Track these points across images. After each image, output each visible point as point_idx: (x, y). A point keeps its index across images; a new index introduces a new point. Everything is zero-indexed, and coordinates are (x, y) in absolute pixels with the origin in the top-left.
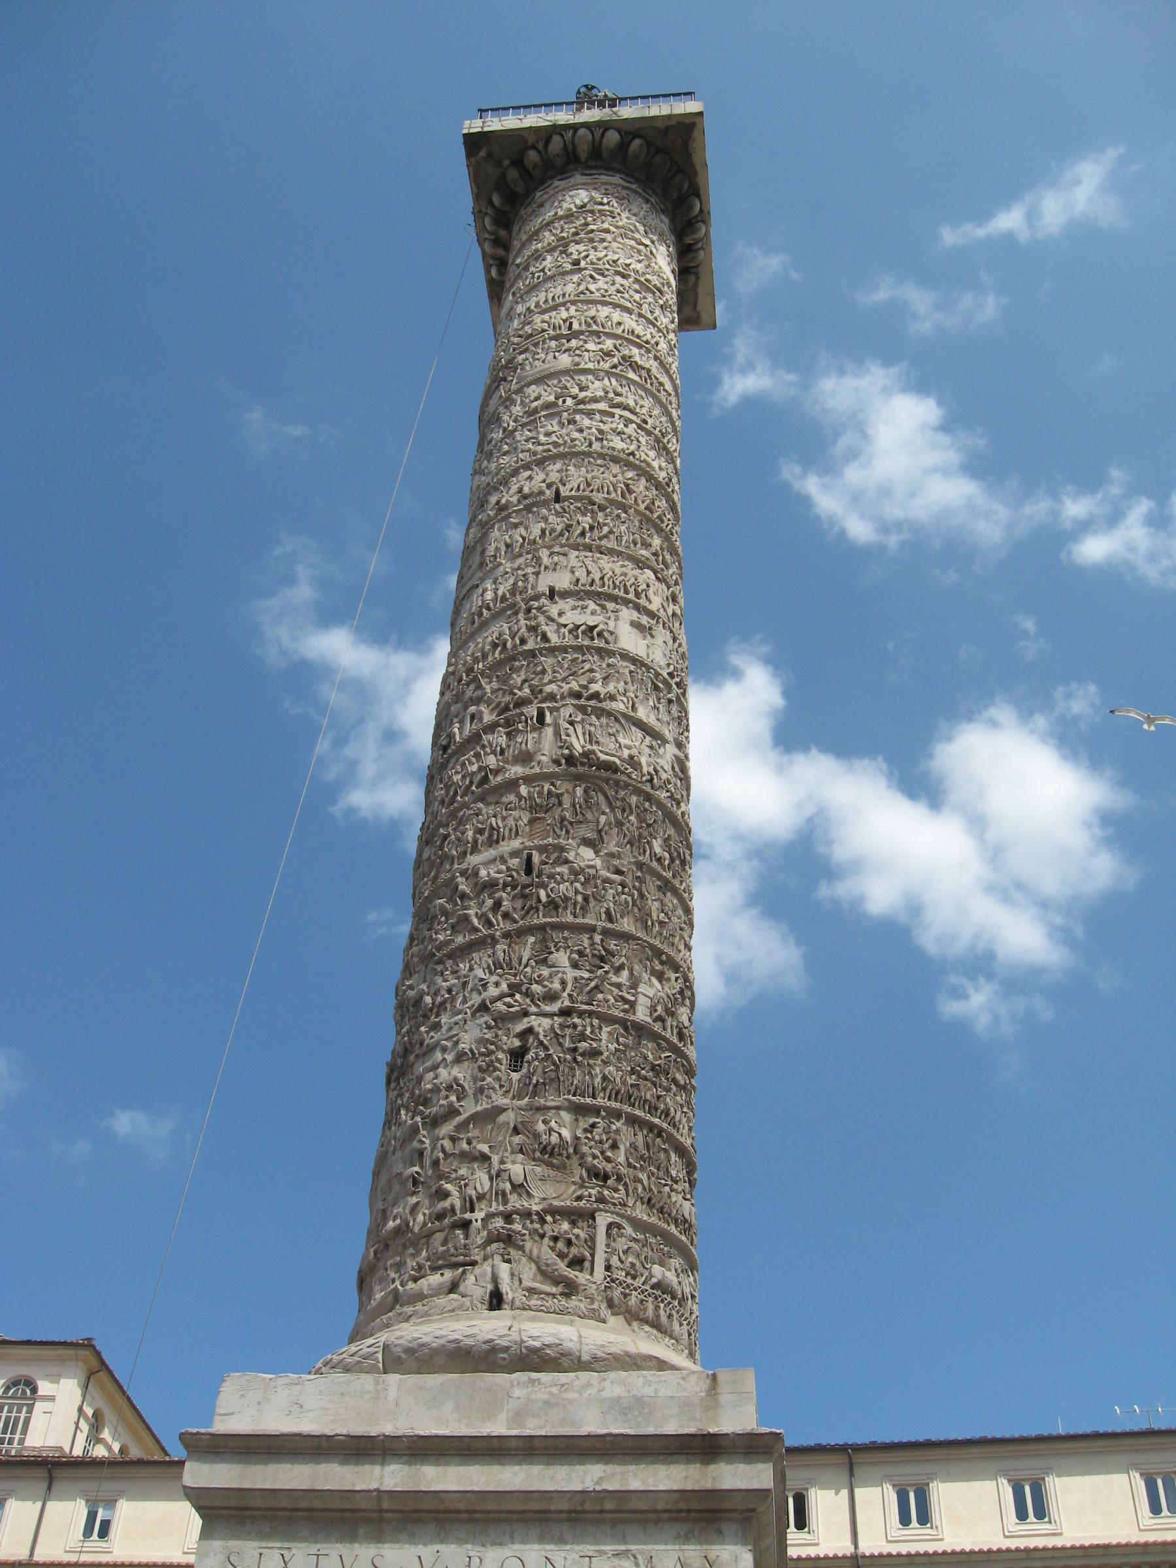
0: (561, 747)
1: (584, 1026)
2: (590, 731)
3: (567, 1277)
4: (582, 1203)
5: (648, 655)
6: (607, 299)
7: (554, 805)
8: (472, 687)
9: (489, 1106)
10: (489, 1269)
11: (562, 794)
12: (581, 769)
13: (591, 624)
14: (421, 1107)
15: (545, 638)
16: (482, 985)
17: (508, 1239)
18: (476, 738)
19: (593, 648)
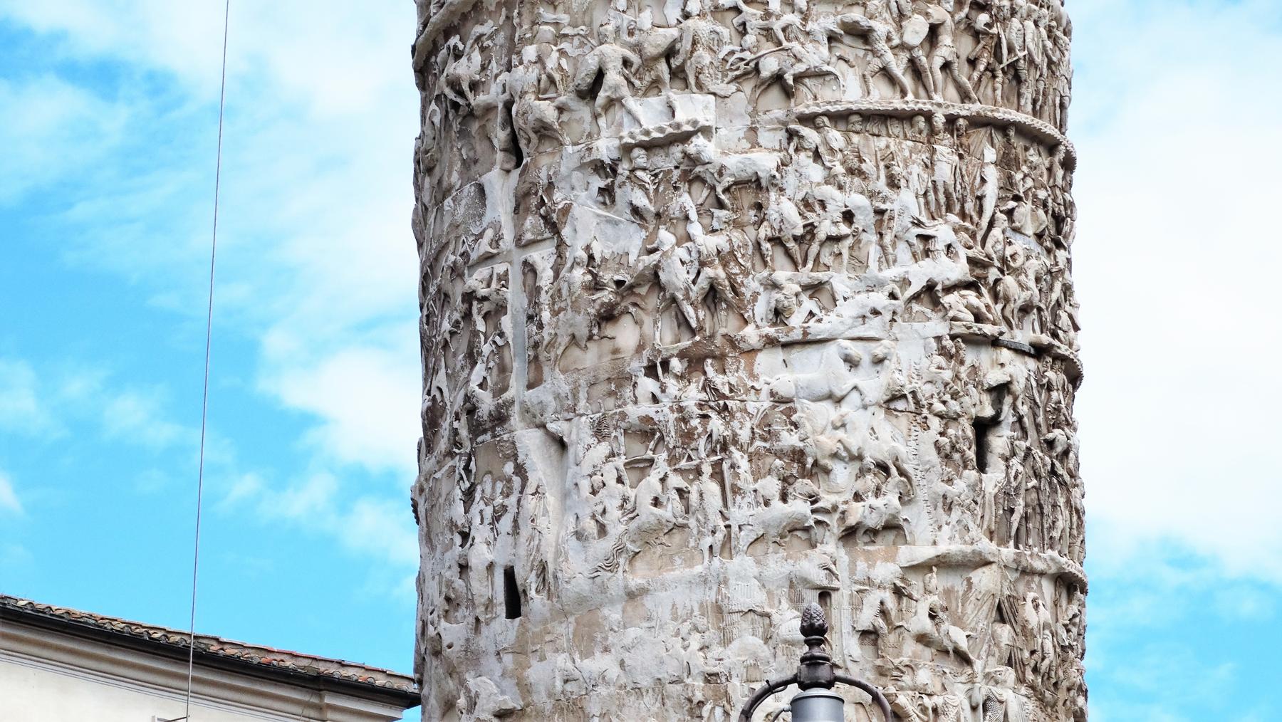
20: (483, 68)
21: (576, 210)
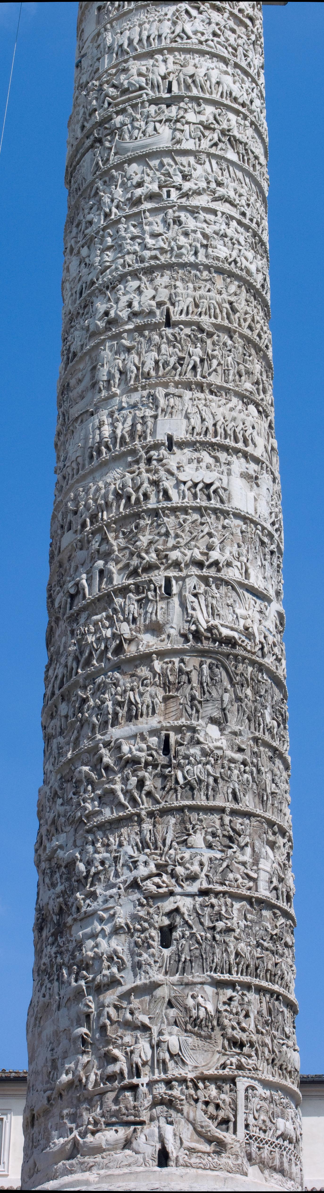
0: (189, 622)
1: (220, 906)
2: (212, 604)
3: (218, 1138)
4: (227, 1072)
5: (256, 510)
6: (204, 47)
7: (185, 683)
8: (98, 537)
9: (147, 981)
10: (156, 1130)
11: (191, 672)
12: (207, 645)
13: (208, 481)
14: (85, 972)
15: (167, 497)
16: (132, 862)
17: (170, 1103)
18: (106, 600)
19: (210, 509)
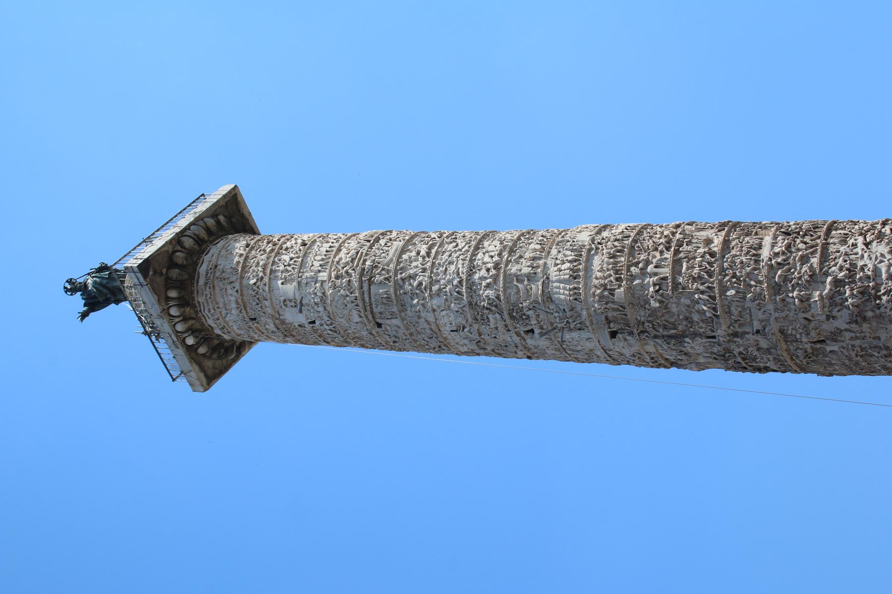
16: (852, 246)
20: (801, 349)
21: (838, 326)
